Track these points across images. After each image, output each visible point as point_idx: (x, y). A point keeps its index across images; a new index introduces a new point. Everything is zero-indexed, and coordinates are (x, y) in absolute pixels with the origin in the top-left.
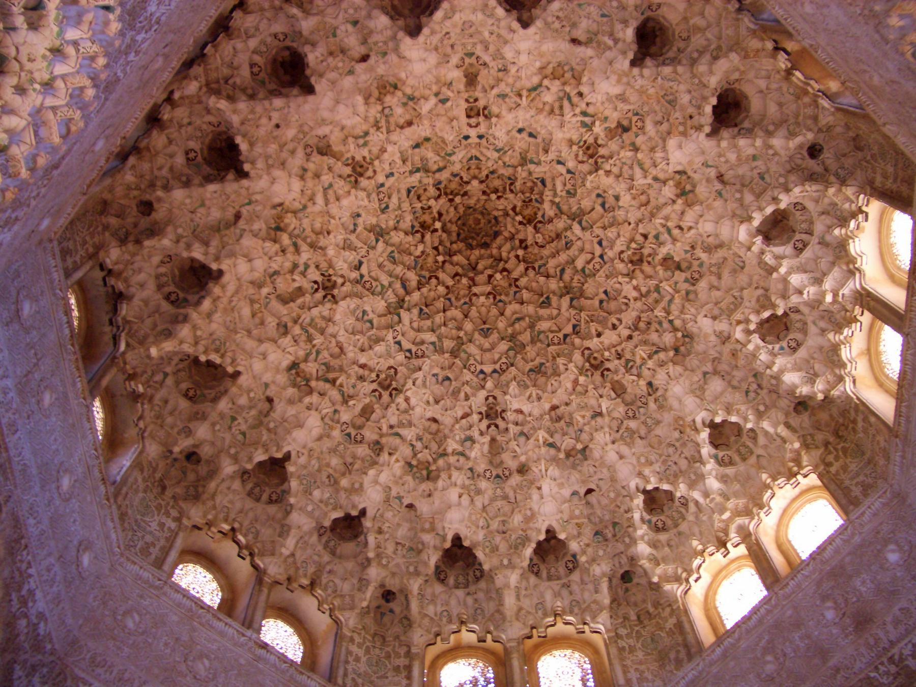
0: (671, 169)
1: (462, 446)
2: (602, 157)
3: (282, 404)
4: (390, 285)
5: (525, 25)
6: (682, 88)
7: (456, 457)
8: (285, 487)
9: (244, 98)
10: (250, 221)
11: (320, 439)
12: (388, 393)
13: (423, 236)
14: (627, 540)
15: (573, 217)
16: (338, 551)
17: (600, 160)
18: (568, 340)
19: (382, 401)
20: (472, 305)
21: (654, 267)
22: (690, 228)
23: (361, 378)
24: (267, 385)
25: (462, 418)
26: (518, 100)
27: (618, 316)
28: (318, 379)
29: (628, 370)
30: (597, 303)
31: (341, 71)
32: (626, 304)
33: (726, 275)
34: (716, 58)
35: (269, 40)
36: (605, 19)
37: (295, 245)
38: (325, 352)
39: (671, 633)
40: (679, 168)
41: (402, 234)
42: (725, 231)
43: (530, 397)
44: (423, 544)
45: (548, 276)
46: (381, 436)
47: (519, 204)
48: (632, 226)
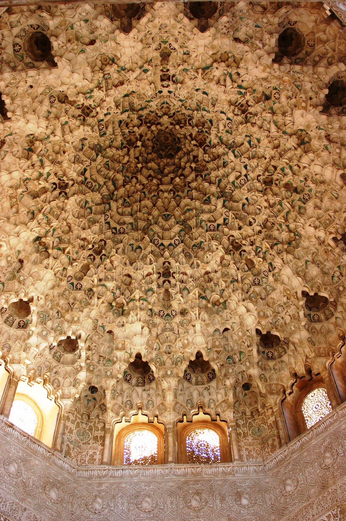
0: (295, 128)
1: (146, 294)
2: (251, 113)
3: (29, 264)
4: (105, 183)
5: (203, 29)
7: (141, 302)
8: (29, 317)
9: (8, 70)
10: (11, 146)
11: (53, 288)
12: (99, 257)
13: (129, 150)
14: (248, 364)
16: (62, 360)
17: (249, 115)
18: (220, 228)
19: (95, 262)
20: (159, 197)
21: (280, 189)
22: (305, 167)
23: (83, 247)
24: (19, 252)
25: (147, 275)
27: (254, 217)
28: (53, 248)
29: (257, 254)
30: (241, 205)
31: (76, 51)
32: (260, 209)
33: (326, 199)
34: (330, 64)
36: (258, 29)
37: (41, 161)
38: (59, 229)
39: (270, 427)
41: (114, 150)
43: (193, 263)
44: (117, 358)
45: (210, 183)
46: (94, 286)
48: (267, 160)
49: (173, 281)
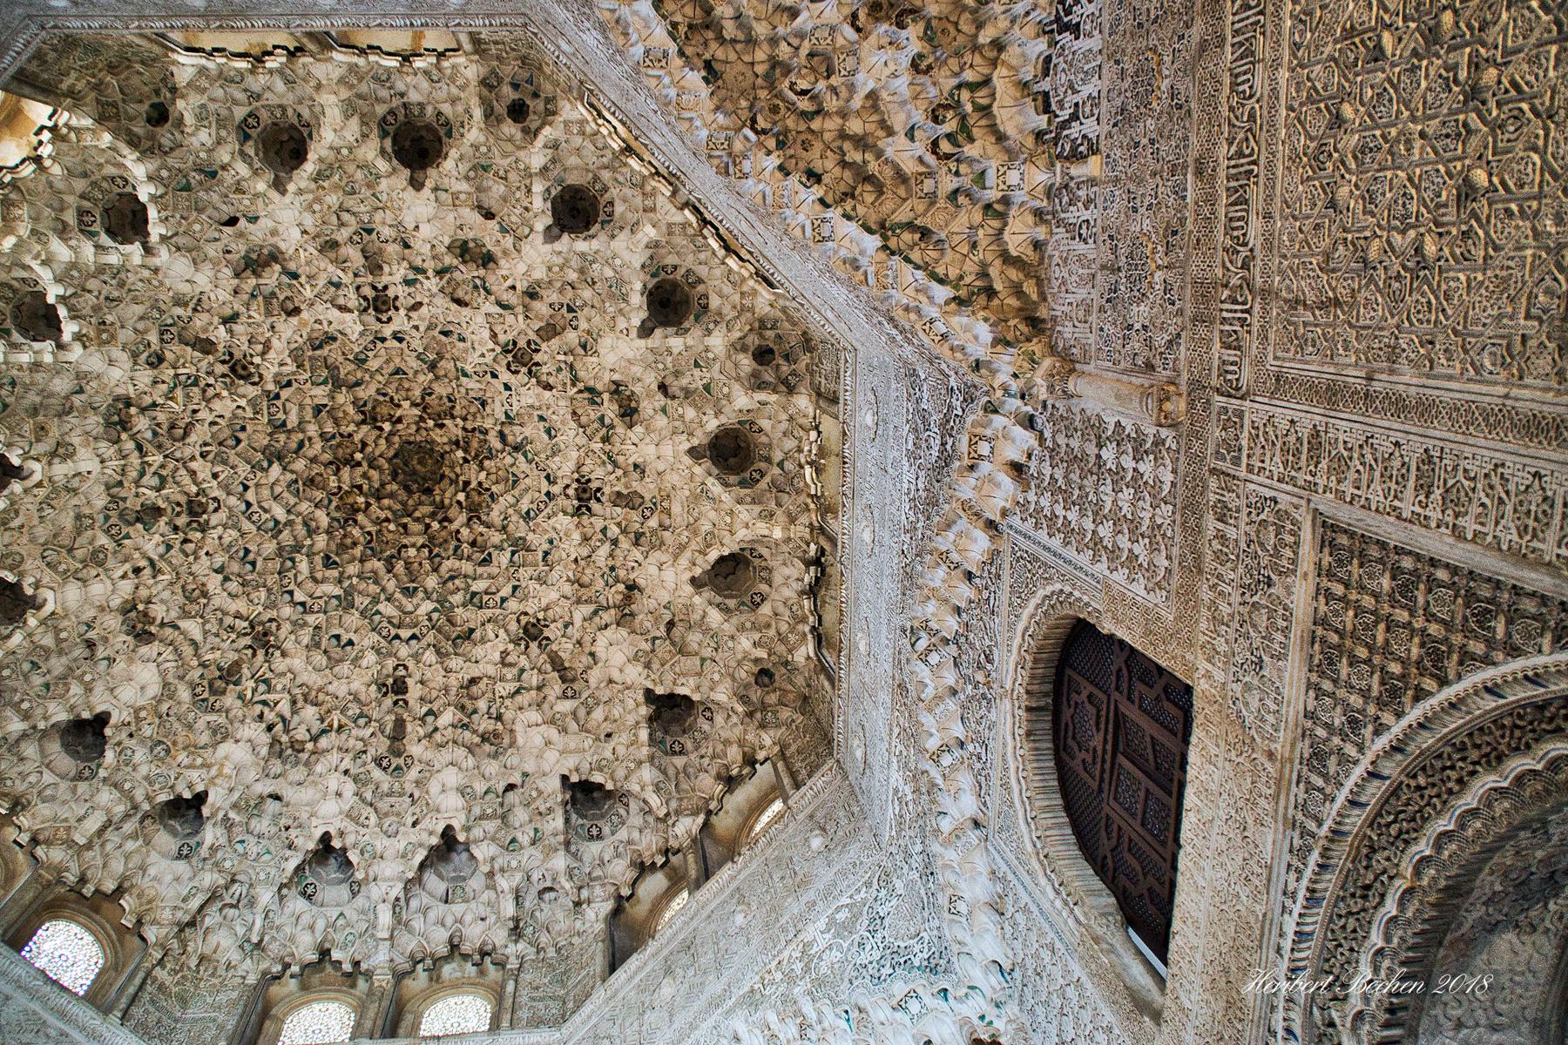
0: (156, 647)
2: (246, 634)
3: (648, 381)
4: (517, 448)
6: (144, 770)
7: (425, 265)
13: (480, 484)
14: (164, 173)
15: (290, 523)
16: (591, 175)
22: (123, 577)
24: (664, 410)
25: (421, 304)
26: (344, 720)
27: (215, 428)
32: (206, 444)
35: (606, 830)
37: (612, 569)
40: (144, 650)
42: (73, 592)
44: (467, 178)
47: (360, 517)
49: (368, 291)
